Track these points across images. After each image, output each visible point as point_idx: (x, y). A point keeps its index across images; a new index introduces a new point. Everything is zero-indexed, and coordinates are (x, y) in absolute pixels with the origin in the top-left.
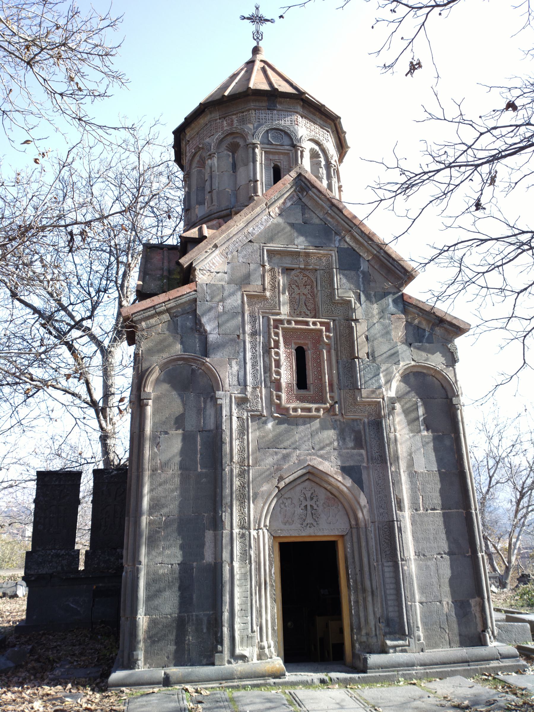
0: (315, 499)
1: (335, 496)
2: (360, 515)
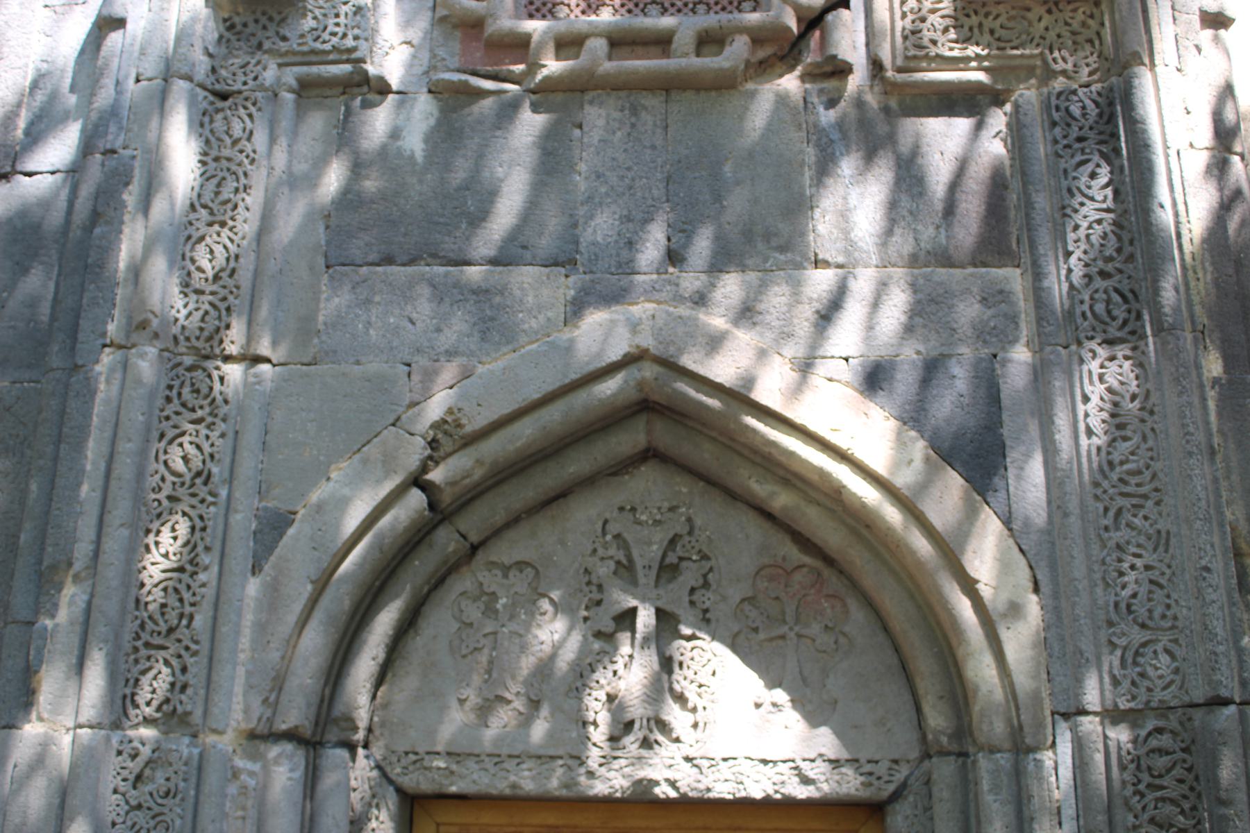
0: (689, 576)
1: (829, 561)
2: (982, 670)
